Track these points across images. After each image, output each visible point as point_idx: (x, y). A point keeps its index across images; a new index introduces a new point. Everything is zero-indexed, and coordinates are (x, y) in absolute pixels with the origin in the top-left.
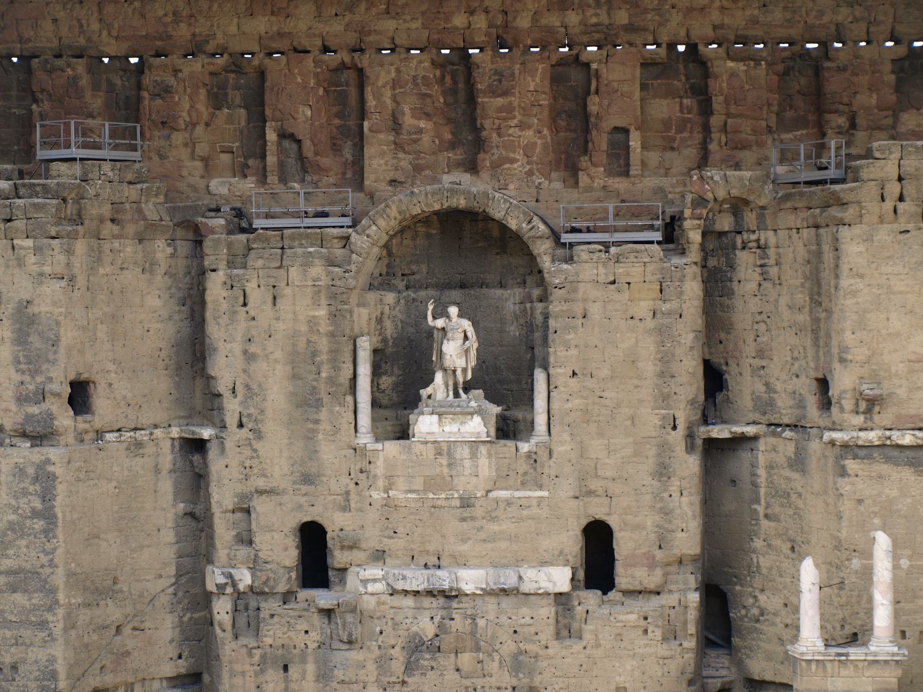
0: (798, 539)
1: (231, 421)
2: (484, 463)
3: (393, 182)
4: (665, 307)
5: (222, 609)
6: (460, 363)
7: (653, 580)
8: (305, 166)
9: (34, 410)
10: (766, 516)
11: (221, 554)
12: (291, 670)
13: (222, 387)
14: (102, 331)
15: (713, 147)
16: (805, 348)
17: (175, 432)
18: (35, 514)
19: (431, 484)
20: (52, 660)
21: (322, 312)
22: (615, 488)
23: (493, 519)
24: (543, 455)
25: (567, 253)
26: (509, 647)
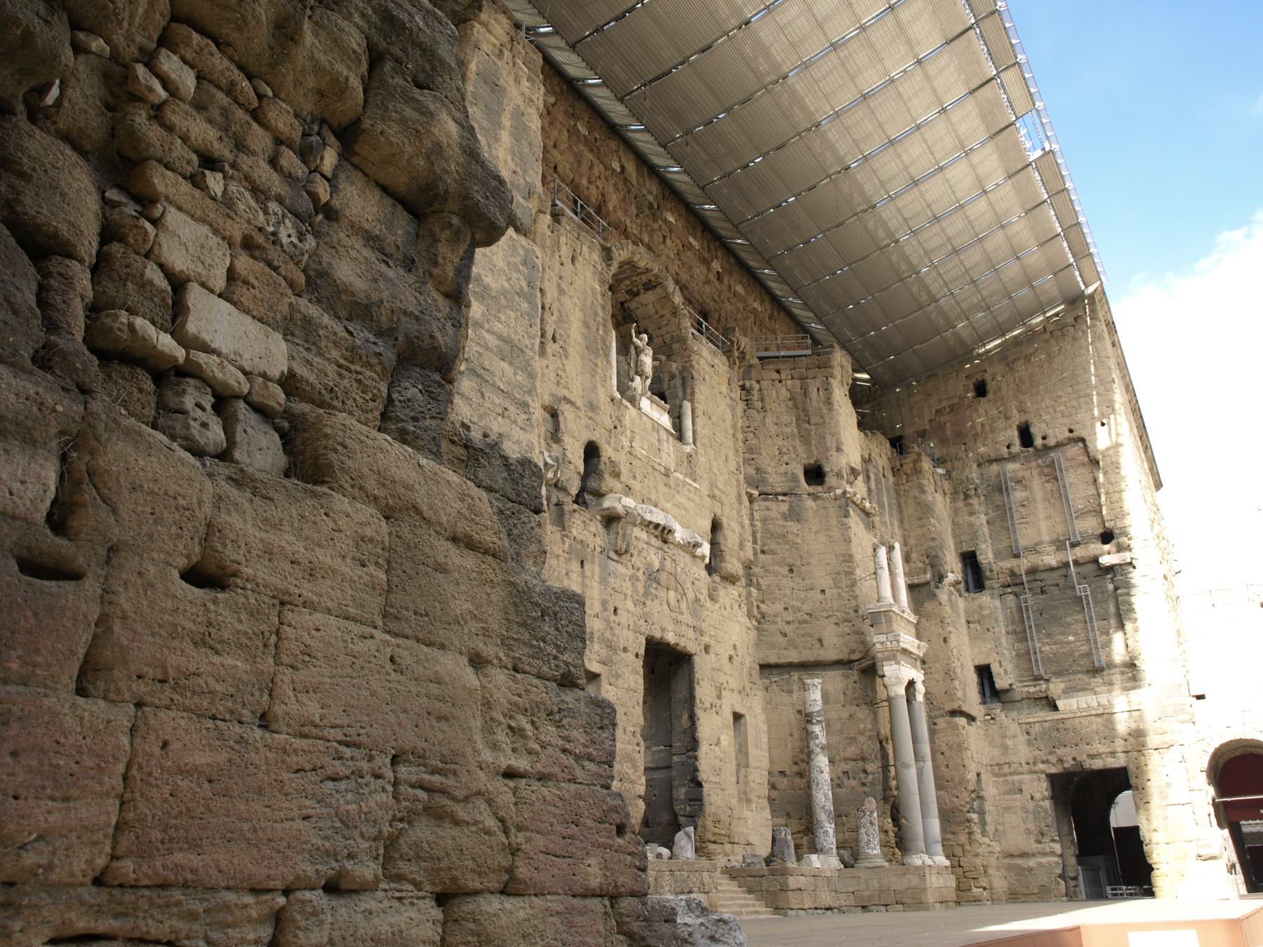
0: (798, 563)
10: (763, 552)
12: (587, 566)
16: (794, 447)
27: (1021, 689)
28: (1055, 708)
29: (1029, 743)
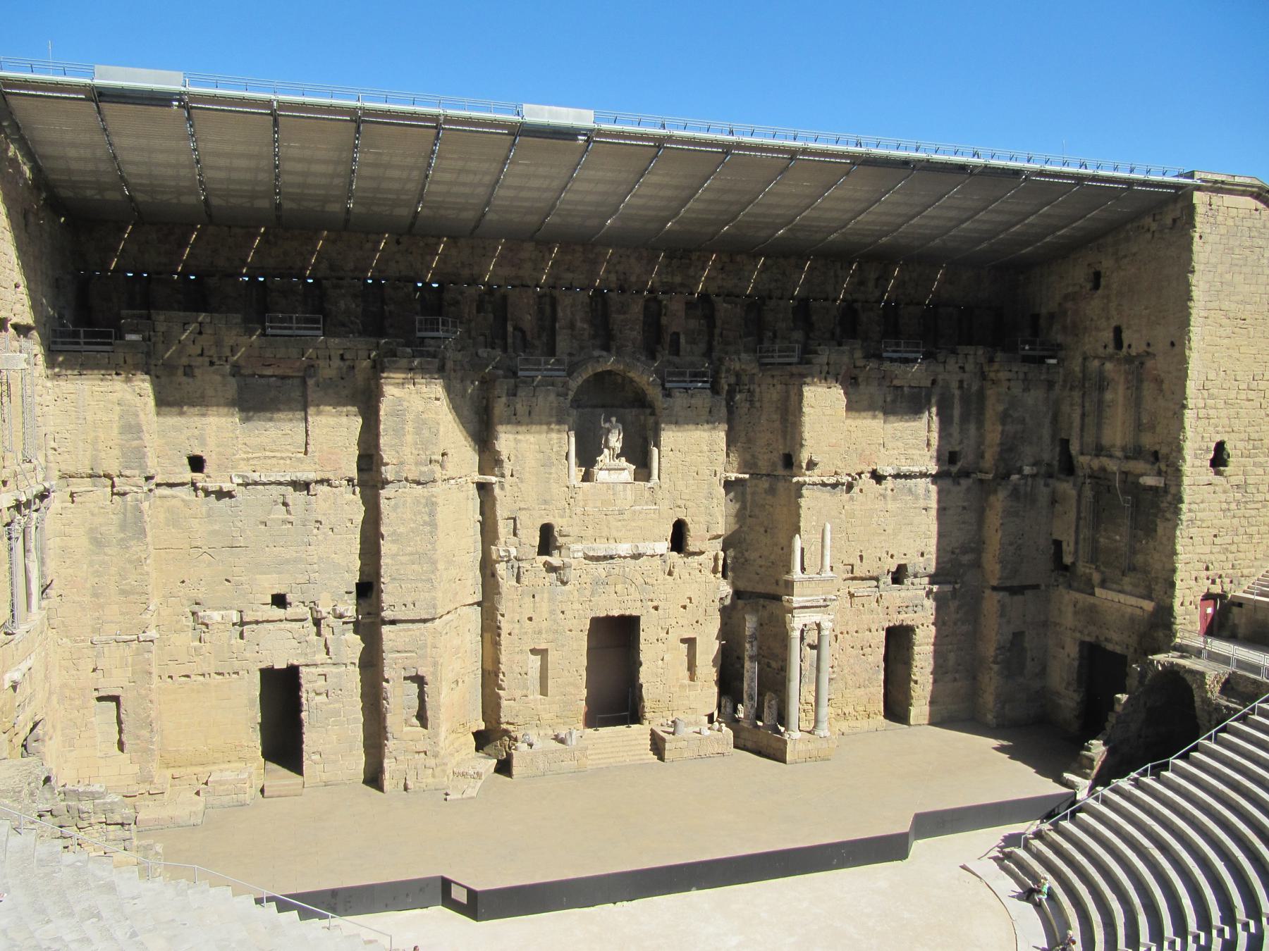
1: (507, 473)
2: (629, 492)
3: (570, 354)
5: (501, 569)
8: (526, 345)
9: (425, 469)
11: (502, 540)
13: (504, 457)
15: (715, 343)
18: (425, 523)
20: (434, 598)
22: (689, 504)
23: (634, 520)
25: (668, 394)
27: (1083, 568)
28: (1093, 594)
29: (1076, 613)
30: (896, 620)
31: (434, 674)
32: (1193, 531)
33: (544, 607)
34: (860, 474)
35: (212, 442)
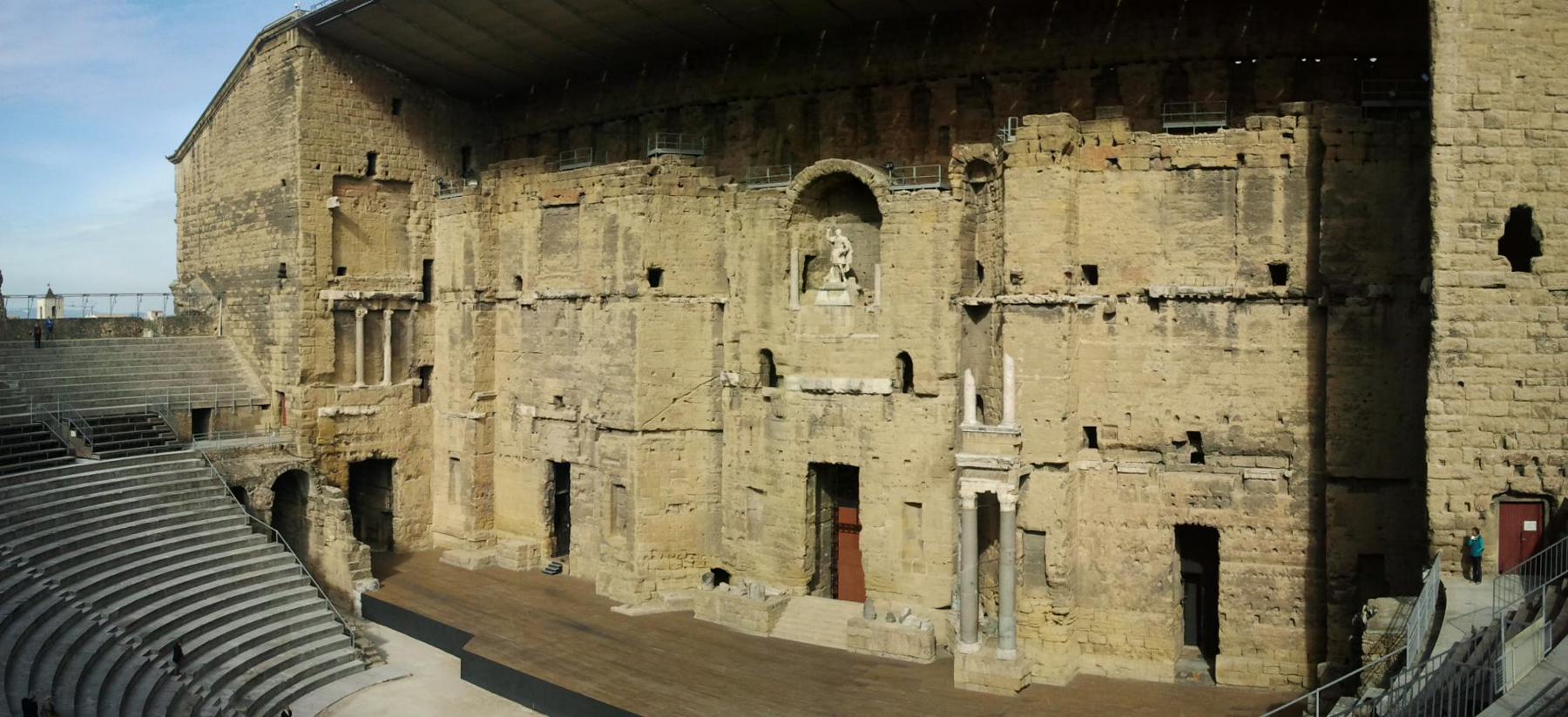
1: (733, 292)
4: (938, 226)
6: (841, 261)
7: (930, 389)
9: (630, 283)
11: (727, 365)
14: (670, 243)
17: (711, 299)
19: (823, 329)
21: (774, 233)
24: (877, 312)
26: (858, 424)
30: (1192, 515)
31: (632, 485)
32: (1465, 372)
33: (762, 441)
34: (1122, 297)
35: (525, 264)
